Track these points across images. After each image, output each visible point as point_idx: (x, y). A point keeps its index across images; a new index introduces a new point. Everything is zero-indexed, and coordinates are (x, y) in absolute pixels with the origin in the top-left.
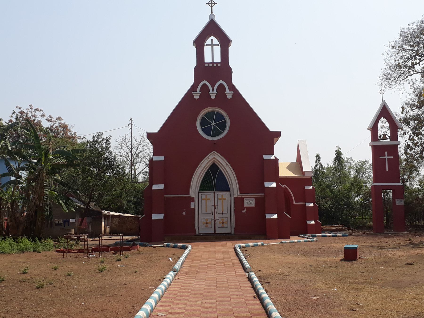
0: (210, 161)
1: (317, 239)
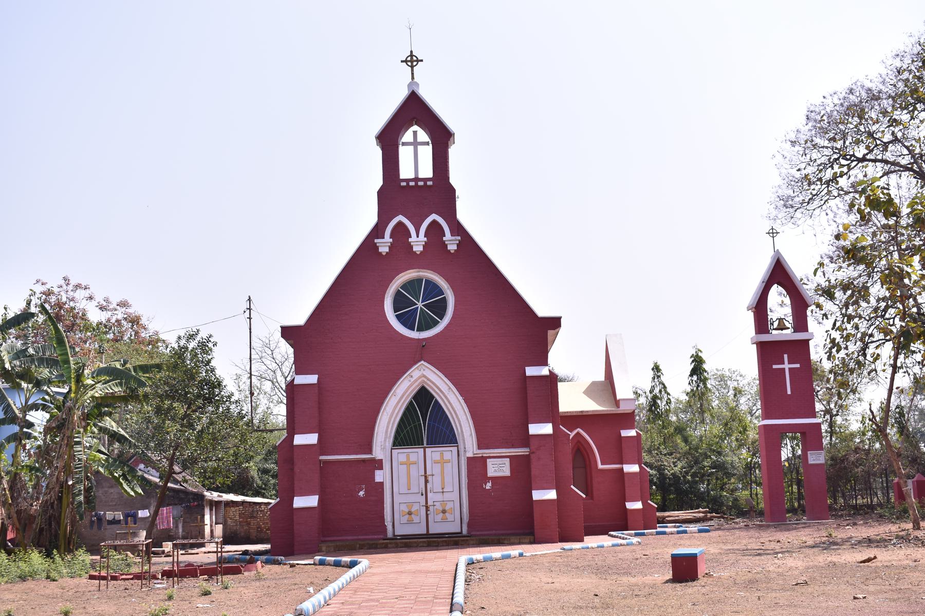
0: (416, 381)
1: (639, 540)
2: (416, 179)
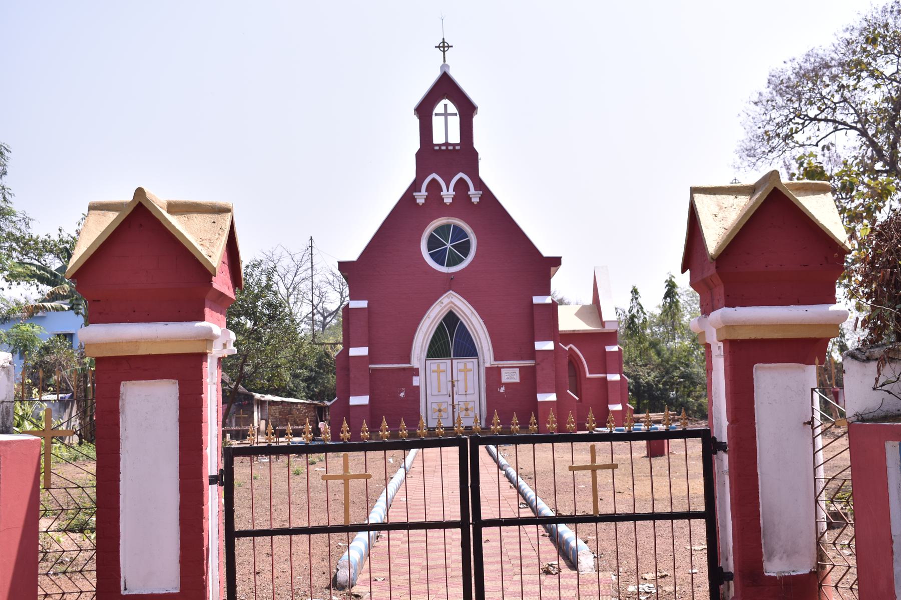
0: (445, 306)
2: (447, 144)
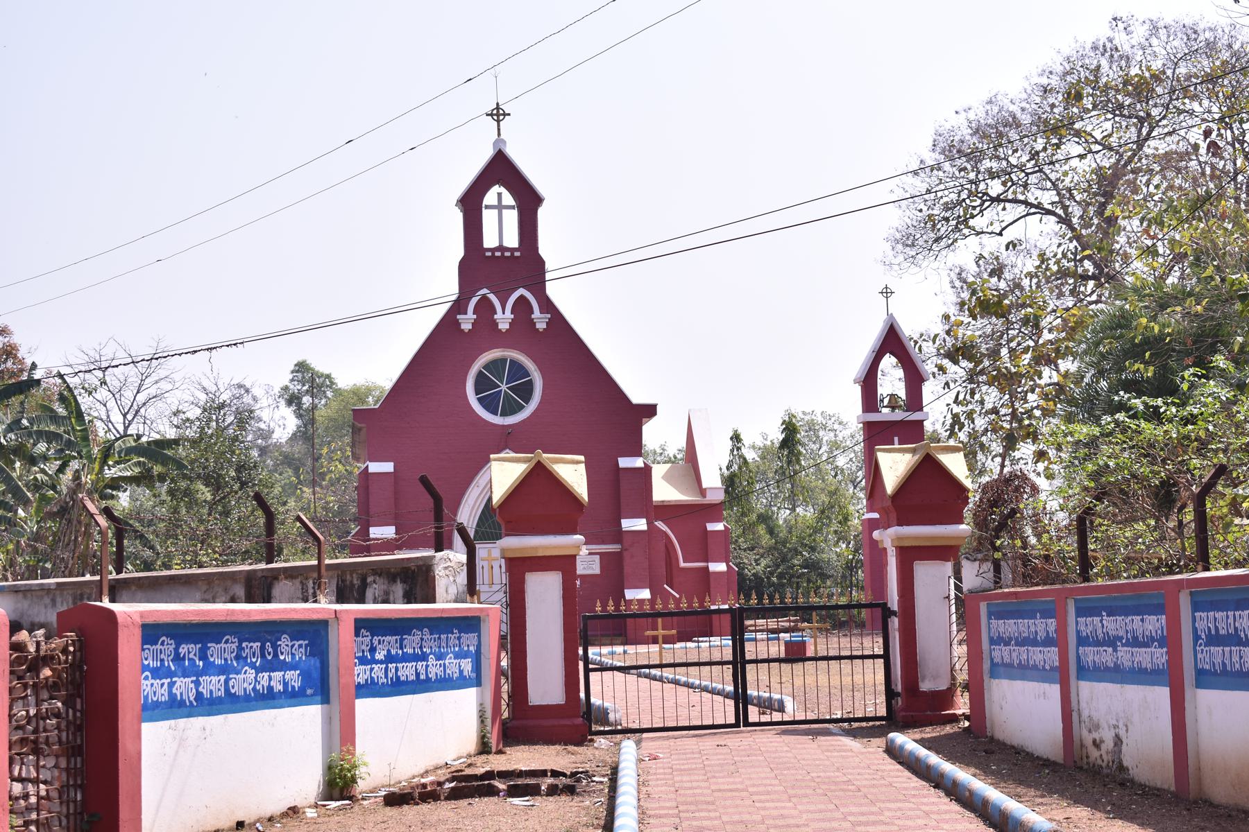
2: (501, 248)
